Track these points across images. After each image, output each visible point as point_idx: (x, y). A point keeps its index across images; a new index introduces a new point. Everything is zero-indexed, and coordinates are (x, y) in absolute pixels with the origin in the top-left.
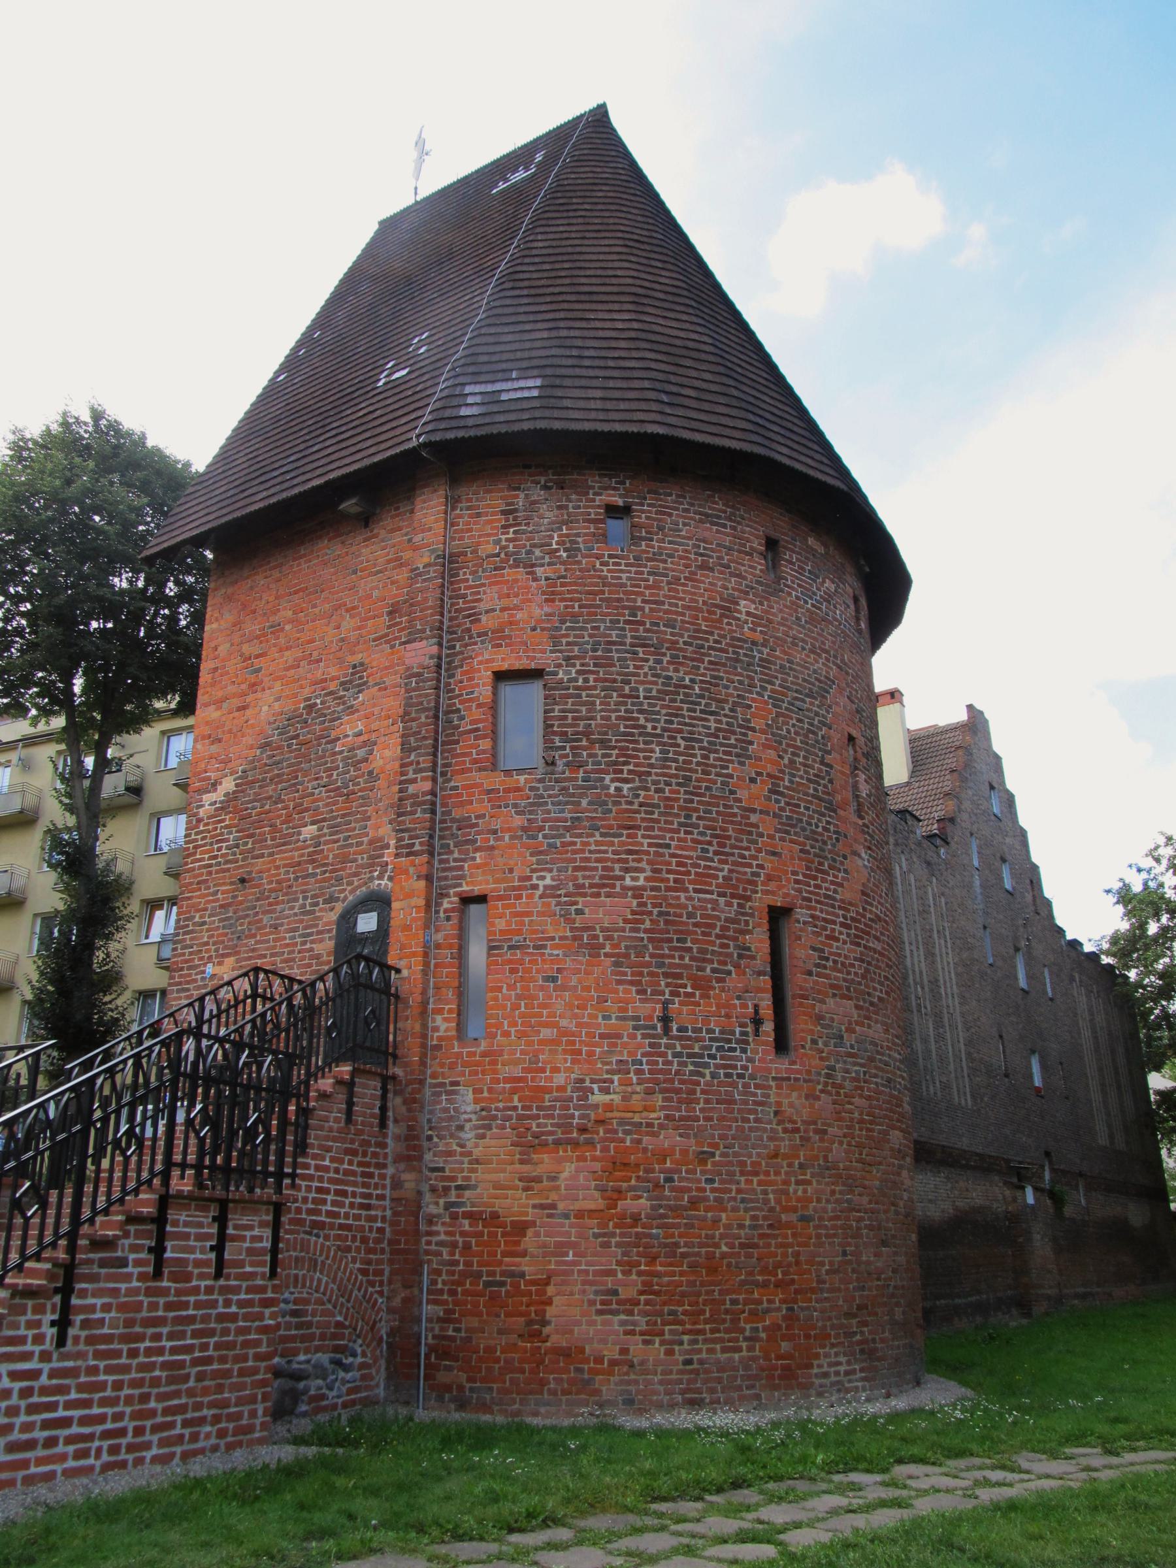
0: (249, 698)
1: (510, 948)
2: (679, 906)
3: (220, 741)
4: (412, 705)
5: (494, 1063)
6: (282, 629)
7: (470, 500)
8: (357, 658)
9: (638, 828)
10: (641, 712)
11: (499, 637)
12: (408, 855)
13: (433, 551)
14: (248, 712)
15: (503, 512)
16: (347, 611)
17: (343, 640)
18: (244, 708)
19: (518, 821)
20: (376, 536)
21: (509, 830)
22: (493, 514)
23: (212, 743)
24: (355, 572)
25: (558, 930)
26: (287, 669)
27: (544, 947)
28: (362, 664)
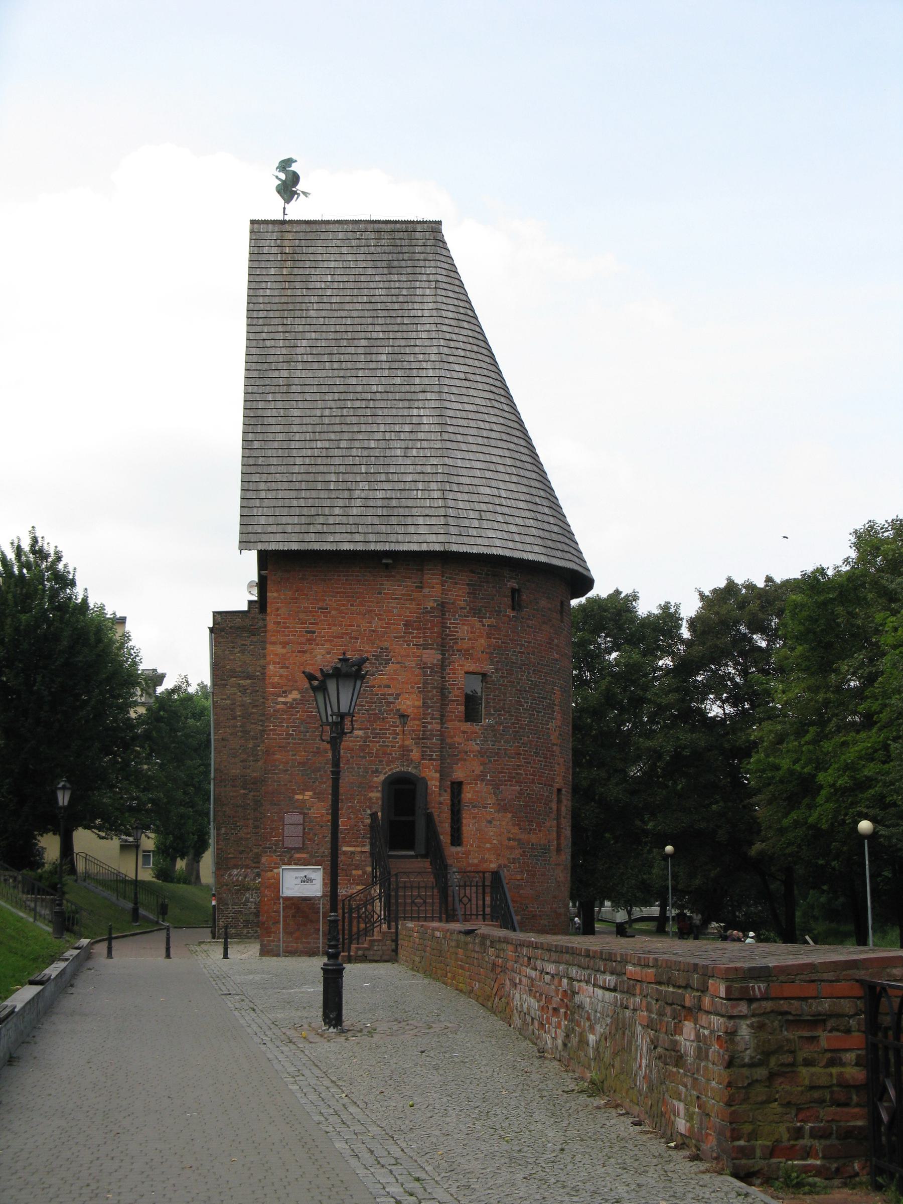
0: (307, 647)
1: (473, 807)
2: (534, 790)
3: (288, 668)
4: (428, 684)
5: (467, 857)
6: (330, 612)
7: (451, 574)
8: (386, 645)
9: (520, 754)
10: (523, 698)
11: (467, 654)
12: (430, 760)
13: (435, 601)
14: (307, 656)
15: (468, 585)
16: (376, 615)
17: (374, 631)
18: (304, 652)
19: (477, 748)
20: (393, 576)
21: (473, 752)
22: (463, 584)
23: (282, 668)
24: (380, 593)
25: (491, 800)
26: (336, 637)
27: (486, 807)
28: (387, 649)
